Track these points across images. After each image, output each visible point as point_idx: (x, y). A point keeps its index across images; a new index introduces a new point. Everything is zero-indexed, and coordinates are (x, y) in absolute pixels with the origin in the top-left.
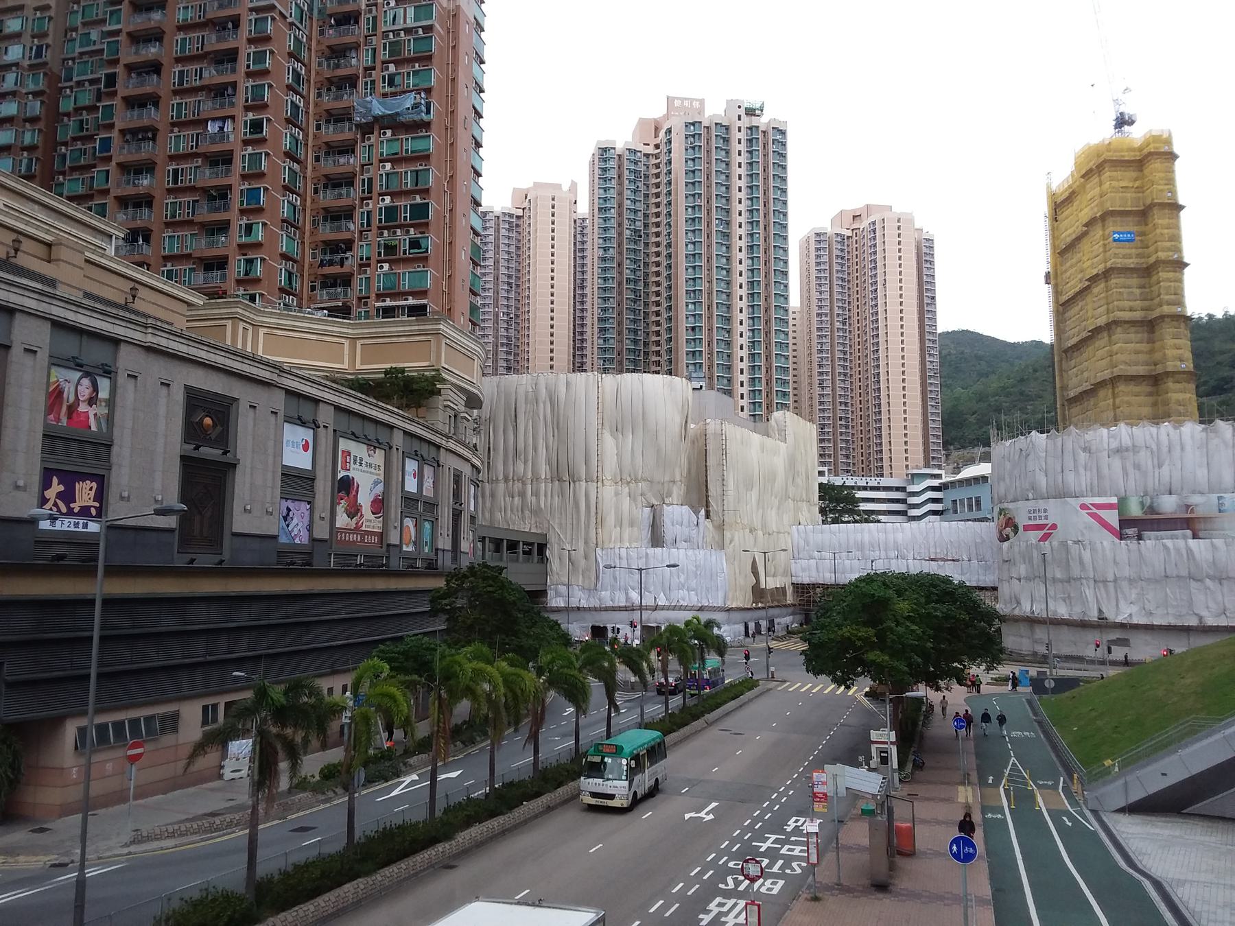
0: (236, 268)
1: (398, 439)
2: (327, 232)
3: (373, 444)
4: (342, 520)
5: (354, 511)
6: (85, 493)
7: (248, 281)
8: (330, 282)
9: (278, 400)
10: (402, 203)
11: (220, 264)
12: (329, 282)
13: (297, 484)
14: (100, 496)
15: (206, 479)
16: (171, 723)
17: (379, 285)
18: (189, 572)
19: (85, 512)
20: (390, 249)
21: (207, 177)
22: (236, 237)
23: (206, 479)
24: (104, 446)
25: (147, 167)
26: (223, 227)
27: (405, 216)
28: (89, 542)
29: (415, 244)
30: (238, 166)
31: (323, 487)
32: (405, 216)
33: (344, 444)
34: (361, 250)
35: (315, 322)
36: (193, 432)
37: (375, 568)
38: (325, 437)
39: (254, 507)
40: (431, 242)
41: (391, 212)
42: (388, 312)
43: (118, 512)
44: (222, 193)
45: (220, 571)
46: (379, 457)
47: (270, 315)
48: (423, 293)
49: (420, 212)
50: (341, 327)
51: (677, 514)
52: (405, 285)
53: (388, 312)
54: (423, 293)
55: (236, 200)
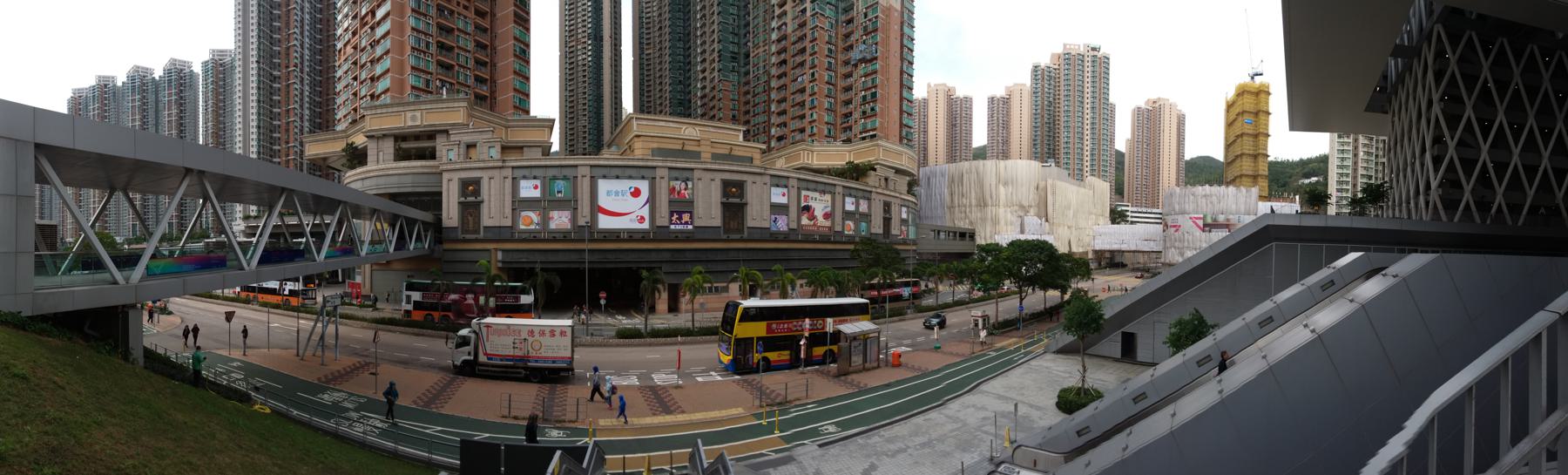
0: (808, 131)
1: (839, 189)
2: (845, 111)
3: (823, 192)
4: (805, 221)
5: (812, 217)
6: (686, 217)
7: (812, 135)
8: (845, 130)
9: (767, 179)
11: (802, 130)
12: (843, 130)
13: (778, 209)
15: (734, 208)
16: (726, 289)
18: (728, 240)
21: (799, 98)
22: (808, 119)
23: (734, 208)
24: (691, 203)
25: (784, 100)
26: (803, 117)
28: (689, 232)
30: (808, 91)
31: (793, 210)
33: (804, 193)
34: (856, 115)
35: (838, 147)
36: (726, 194)
37: (825, 239)
38: (794, 192)
41: (864, 97)
43: (698, 223)
44: (802, 104)
45: (742, 240)
46: (828, 197)
47: (817, 147)
49: (874, 95)
50: (847, 147)
55: (808, 105)
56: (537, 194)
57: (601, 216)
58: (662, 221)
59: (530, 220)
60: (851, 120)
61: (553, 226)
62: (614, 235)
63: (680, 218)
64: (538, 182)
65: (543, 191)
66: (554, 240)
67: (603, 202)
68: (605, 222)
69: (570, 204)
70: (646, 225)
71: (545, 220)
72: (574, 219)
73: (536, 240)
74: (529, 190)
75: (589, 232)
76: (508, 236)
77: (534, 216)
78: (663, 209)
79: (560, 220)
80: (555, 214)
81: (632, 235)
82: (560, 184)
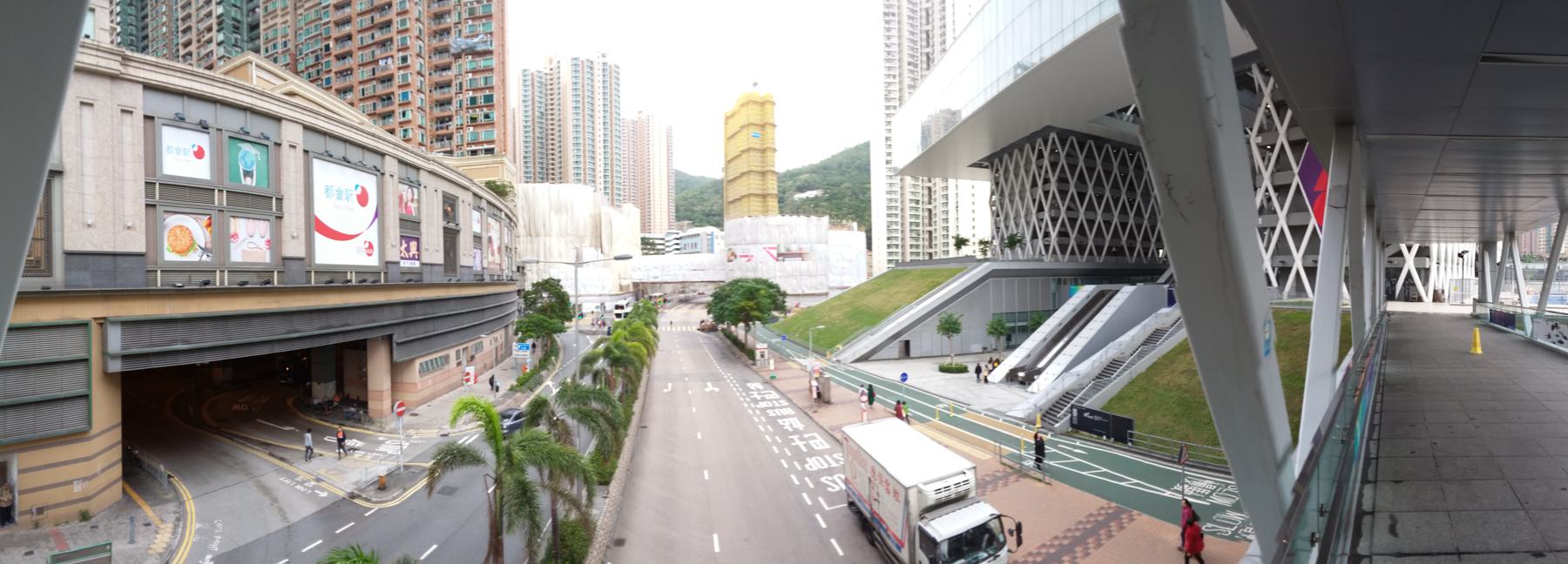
10: (478, 94)
14: (418, 249)
17: (468, 138)
19: (413, 258)
20: (473, 119)
27: (481, 101)
29: (487, 116)
32: (481, 101)
39: (468, 257)
40: (495, 115)
41: (473, 100)
42: (474, 153)
43: (425, 259)
45: (459, 285)
48: (492, 142)
49: (489, 99)
51: (589, 253)
52: (482, 138)
53: (474, 153)
54: (492, 142)
56: (201, 171)
57: (319, 239)
58: (393, 255)
59: (186, 238)
60: (453, 126)
61: (237, 255)
62: (335, 279)
63: (408, 250)
64: (203, 140)
65: (218, 166)
66: (242, 291)
67: (325, 210)
68: (328, 253)
69: (262, 203)
70: (373, 261)
71: (222, 240)
72: (275, 242)
73: (206, 291)
74: (184, 157)
75: (289, 274)
76: (137, 282)
77: (196, 227)
78: (394, 231)
79: (250, 242)
80: (239, 226)
81: (367, 280)
82: (250, 155)
